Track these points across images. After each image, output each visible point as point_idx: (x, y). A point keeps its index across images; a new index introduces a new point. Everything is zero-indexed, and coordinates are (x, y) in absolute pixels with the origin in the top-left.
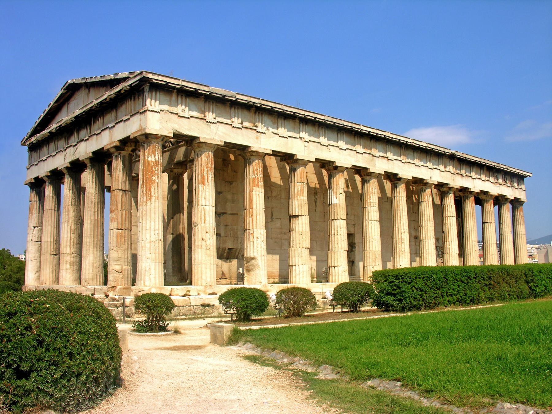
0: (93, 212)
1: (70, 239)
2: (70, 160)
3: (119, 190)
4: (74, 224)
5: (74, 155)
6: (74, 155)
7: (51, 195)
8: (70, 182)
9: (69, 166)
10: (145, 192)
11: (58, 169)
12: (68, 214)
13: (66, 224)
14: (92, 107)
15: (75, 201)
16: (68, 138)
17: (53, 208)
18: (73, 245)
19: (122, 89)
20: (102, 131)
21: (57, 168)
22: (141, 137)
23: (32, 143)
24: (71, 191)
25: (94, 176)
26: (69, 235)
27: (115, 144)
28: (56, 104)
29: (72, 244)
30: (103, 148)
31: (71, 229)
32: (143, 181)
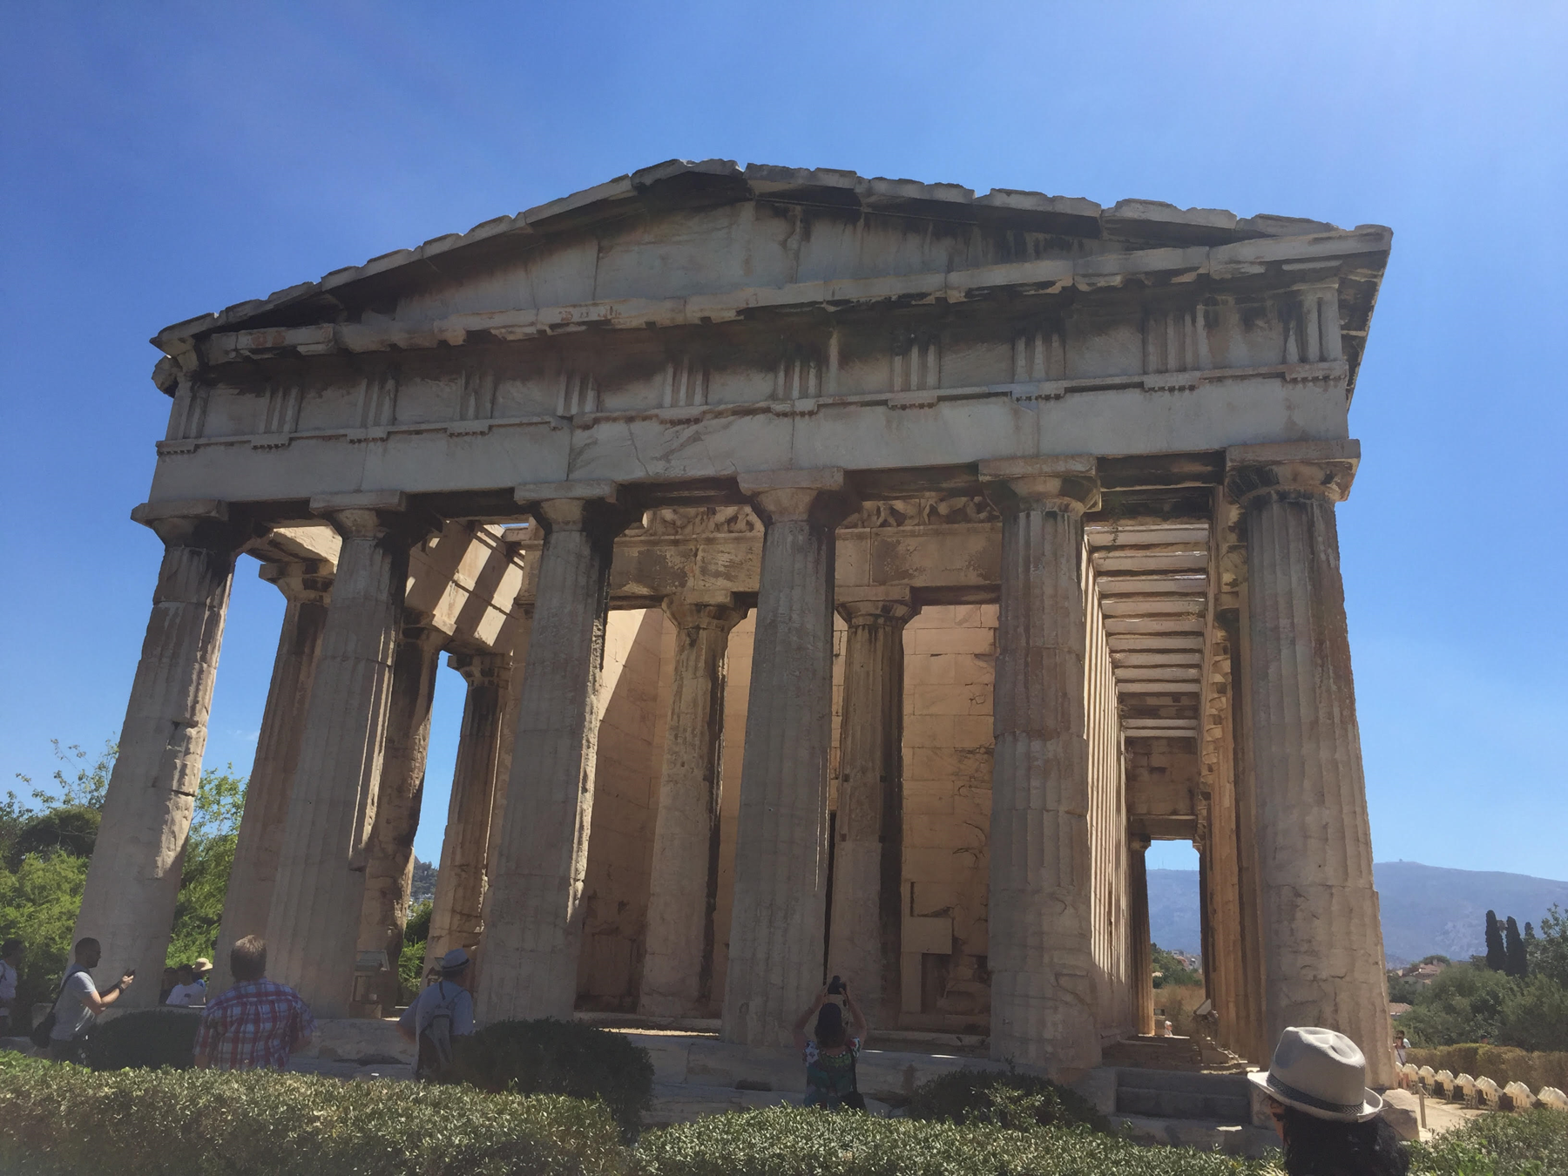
2: (637, 473)
5: (666, 457)
6: (666, 457)
7: (384, 596)
9: (612, 500)
10: (1334, 688)
11: (521, 496)
14: (923, 295)
16: (608, 382)
19: (1196, 269)
20: (941, 399)
21: (511, 490)
22: (1306, 471)
23: (291, 351)
27: (1078, 467)
28: (530, 231)
30: (973, 468)
32: (1320, 643)
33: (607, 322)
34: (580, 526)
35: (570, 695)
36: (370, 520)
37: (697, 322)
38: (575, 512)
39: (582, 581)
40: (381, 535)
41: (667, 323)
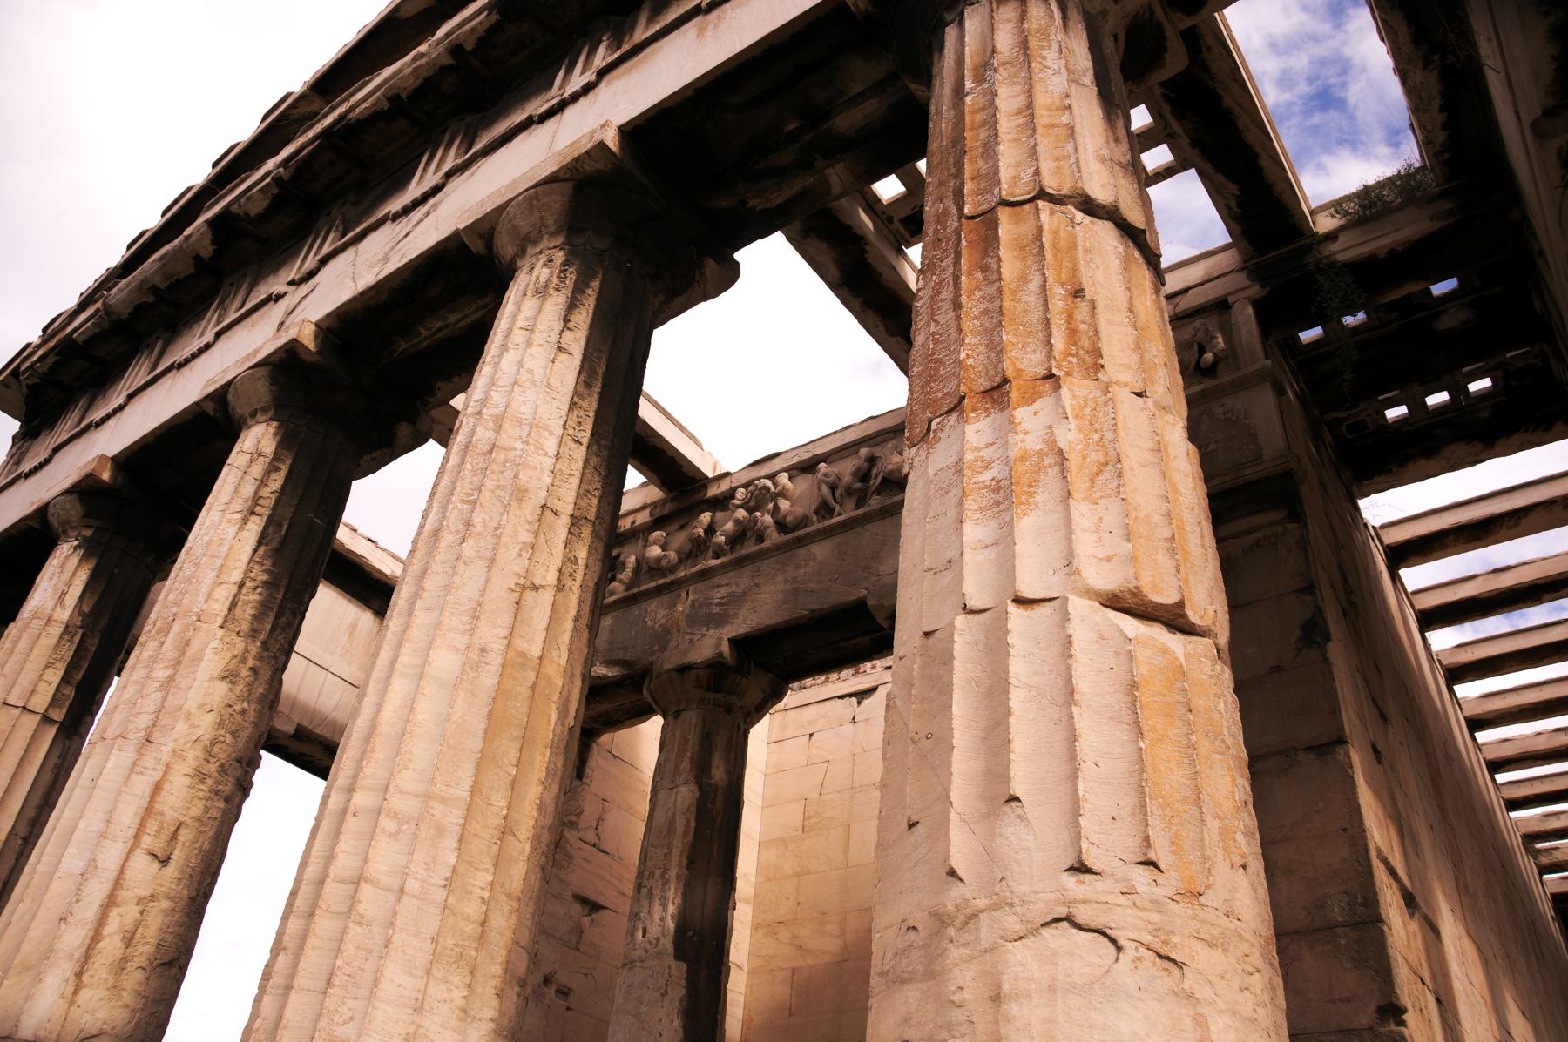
0: (502, 583)
1: (110, 902)
3: (1089, 206)
4: (200, 776)
7: (64, 615)
8: (272, 468)
12: (168, 685)
13: (129, 754)
15: (264, 606)
17: (41, 702)
18: (122, 965)
24: (255, 526)
25: (583, 317)
26: (111, 856)
29: (111, 945)
31: (149, 811)
33: (342, 117)
34: (271, 413)
35: (161, 674)
36: (74, 509)
37: (448, 61)
38: (262, 391)
39: (249, 489)
40: (87, 533)
41: (412, 83)
